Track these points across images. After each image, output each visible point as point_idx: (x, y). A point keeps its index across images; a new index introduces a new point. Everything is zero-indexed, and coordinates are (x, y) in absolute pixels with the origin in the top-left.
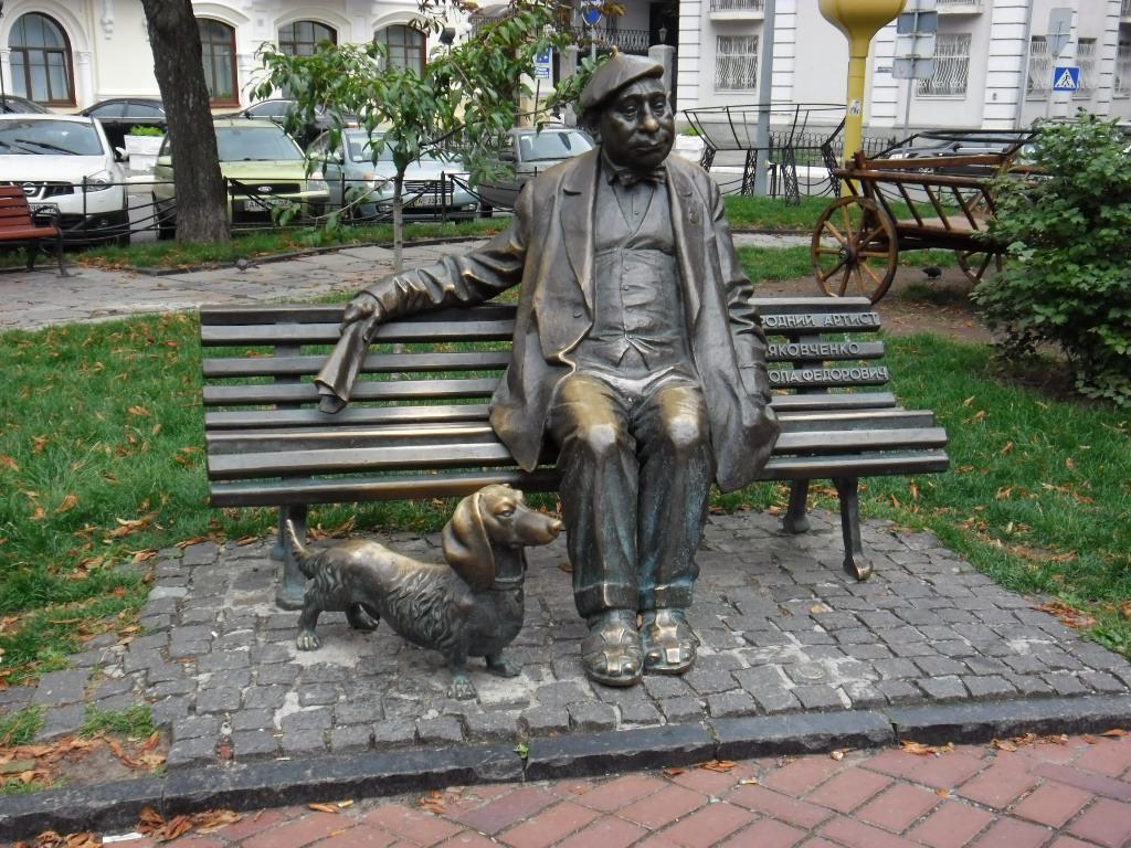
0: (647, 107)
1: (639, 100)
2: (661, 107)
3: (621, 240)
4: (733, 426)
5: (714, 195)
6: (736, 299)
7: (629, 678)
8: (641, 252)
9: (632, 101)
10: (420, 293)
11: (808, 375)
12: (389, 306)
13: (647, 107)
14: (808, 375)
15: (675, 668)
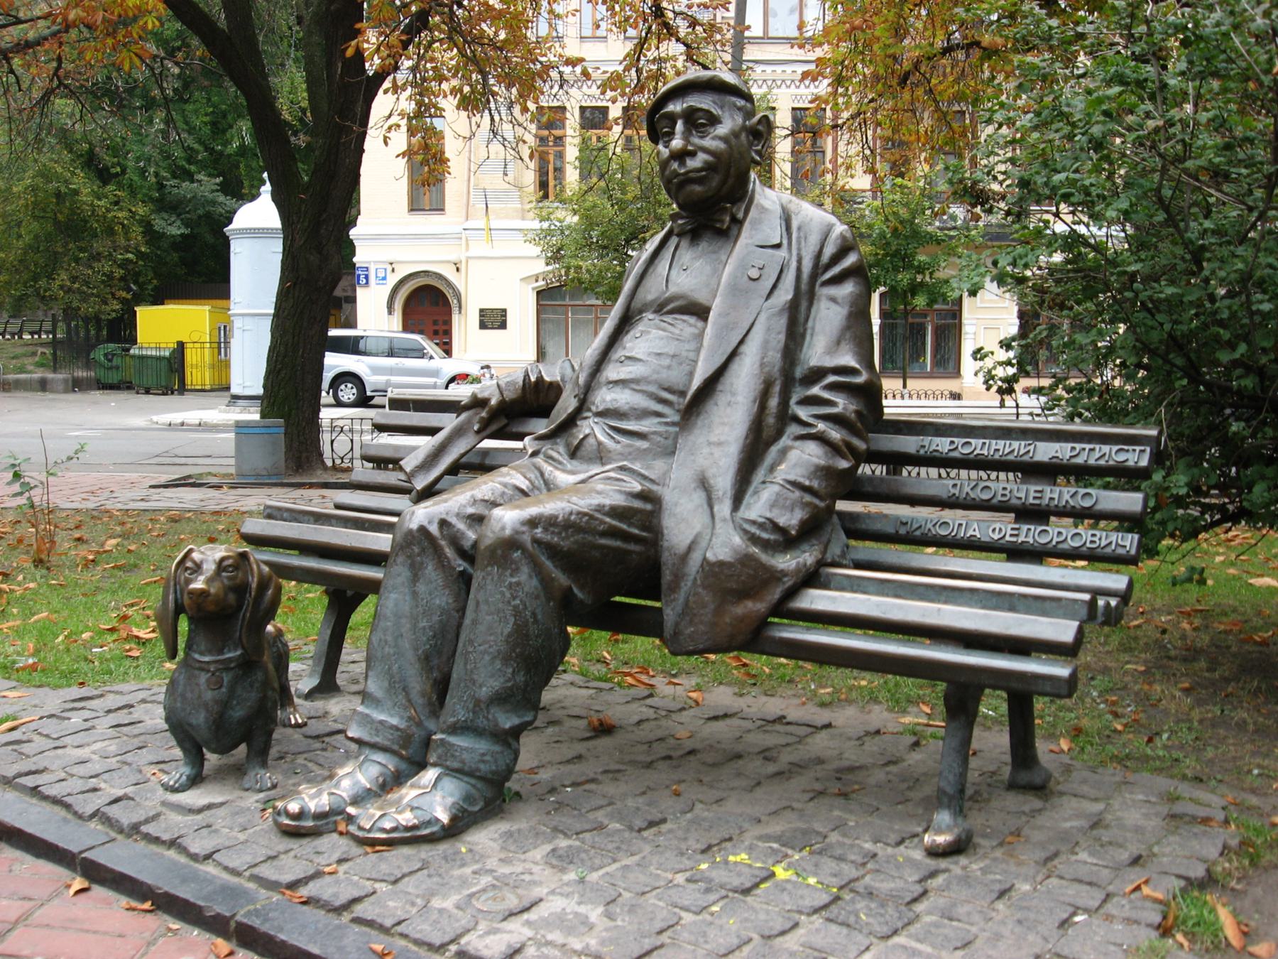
0: (679, 126)
1: (672, 118)
2: (703, 125)
3: (653, 301)
4: (696, 558)
5: (829, 251)
6: (816, 390)
7: (287, 821)
8: (668, 318)
9: (664, 122)
10: (551, 383)
11: (1030, 534)
12: (509, 395)
13: (679, 126)
14: (1030, 534)
15: (361, 834)
